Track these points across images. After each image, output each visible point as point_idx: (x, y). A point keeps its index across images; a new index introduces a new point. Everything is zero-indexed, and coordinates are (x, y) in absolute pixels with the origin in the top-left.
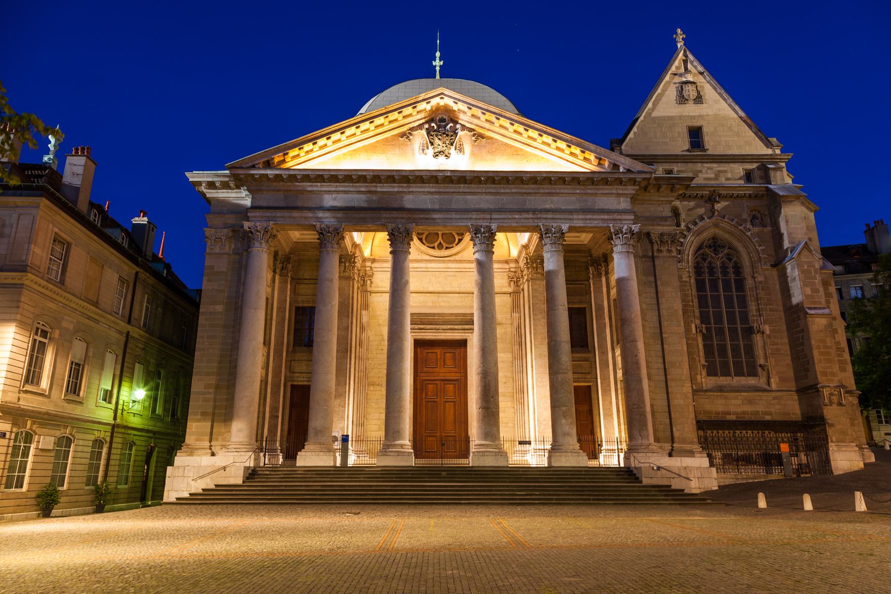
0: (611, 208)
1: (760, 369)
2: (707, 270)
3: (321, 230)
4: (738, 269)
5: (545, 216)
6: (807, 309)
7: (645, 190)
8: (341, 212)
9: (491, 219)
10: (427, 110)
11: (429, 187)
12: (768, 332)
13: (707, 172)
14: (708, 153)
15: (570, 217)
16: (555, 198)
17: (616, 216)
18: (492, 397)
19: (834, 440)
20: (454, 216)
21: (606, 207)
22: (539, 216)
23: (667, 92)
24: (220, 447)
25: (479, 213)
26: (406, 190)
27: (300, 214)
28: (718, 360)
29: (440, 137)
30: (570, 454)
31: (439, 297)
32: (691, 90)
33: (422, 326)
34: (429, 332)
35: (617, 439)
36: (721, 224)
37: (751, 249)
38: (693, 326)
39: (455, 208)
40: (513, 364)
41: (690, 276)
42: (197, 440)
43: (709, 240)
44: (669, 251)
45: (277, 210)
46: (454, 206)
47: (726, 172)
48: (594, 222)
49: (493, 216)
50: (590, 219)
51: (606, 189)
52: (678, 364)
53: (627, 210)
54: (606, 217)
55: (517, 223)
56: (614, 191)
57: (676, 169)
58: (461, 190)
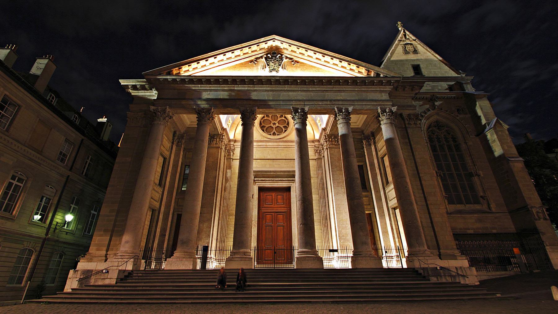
4: (454, 139)
7: (396, 90)
9: (305, 105)
10: (266, 48)
12: (482, 176)
16: (343, 94)
18: (309, 217)
19: (548, 244)
20: (281, 103)
21: (374, 98)
22: (334, 103)
23: (397, 49)
25: (297, 101)
26: (252, 89)
29: (273, 61)
30: (369, 258)
31: (273, 162)
32: (410, 48)
33: (263, 179)
34: (267, 183)
35: (398, 247)
36: (440, 113)
40: (319, 201)
42: (98, 250)
46: (281, 98)
47: (437, 86)
48: (367, 106)
50: (365, 105)
51: (373, 88)
54: (375, 103)
56: (378, 89)
58: (286, 89)
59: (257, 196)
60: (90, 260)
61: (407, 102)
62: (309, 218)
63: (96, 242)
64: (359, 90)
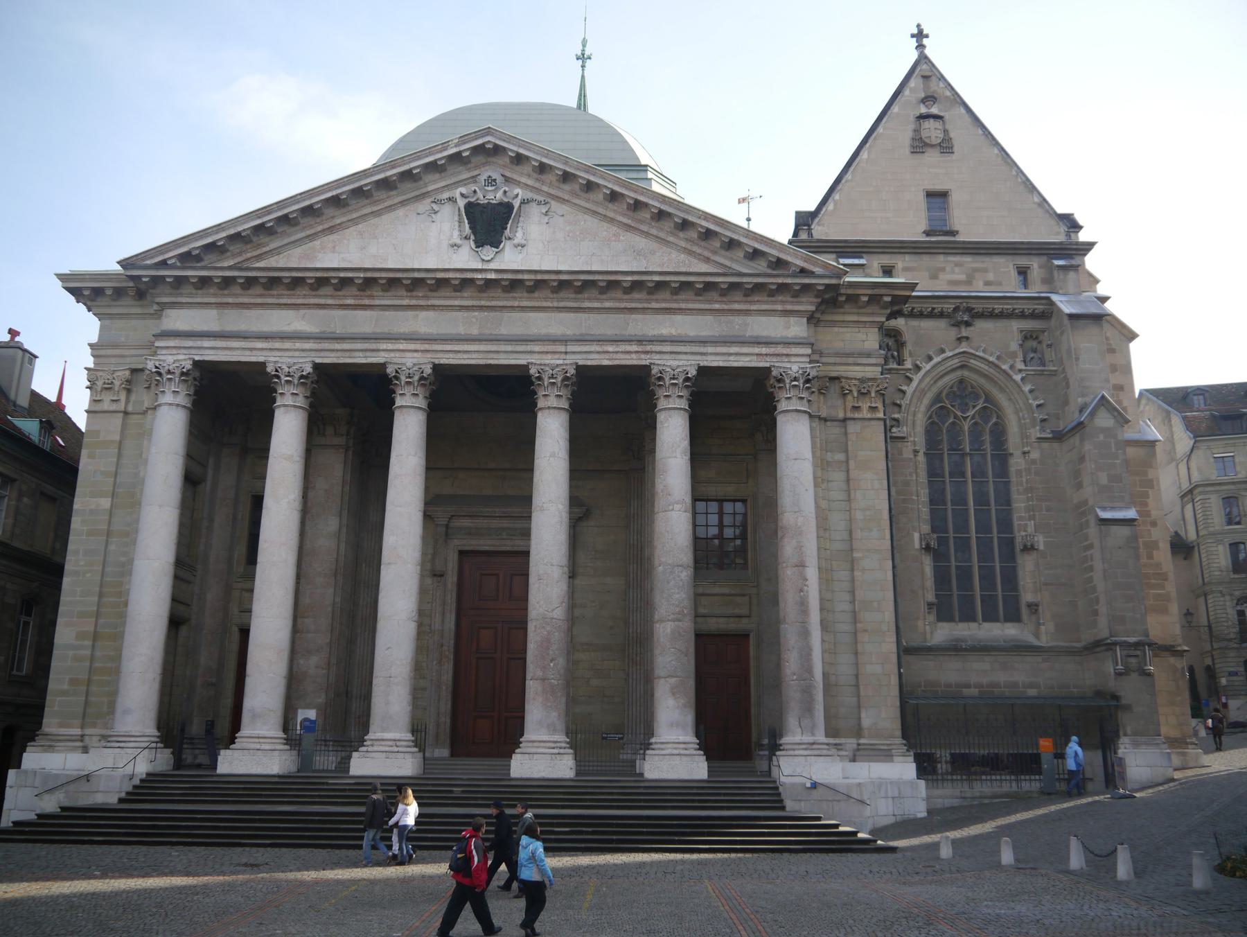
0: (773, 335)
1: (1024, 612)
2: (945, 437)
3: (277, 371)
5: (658, 348)
6: (1098, 510)
8: (312, 341)
9: (566, 353)
11: (462, 297)
12: (1042, 547)
13: (953, 272)
14: (959, 238)
15: (702, 350)
17: (780, 350)
18: (552, 661)
19: (1129, 731)
22: (648, 348)
24: (98, 738)
25: (547, 343)
26: (422, 302)
27: (243, 343)
28: (955, 592)
37: (1022, 405)
38: (916, 536)
39: (505, 333)
41: (916, 452)
42: (61, 725)
43: (951, 387)
44: (873, 409)
45: (205, 338)
48: (743, 358)
49: (570, 348)
50: (736, 354)
52: (875, 604)
53: (801, 338)
54: (764, 350)
55: (610, 359)
56: (779, 307)
57: (900, 265)
58: (516, 304)
59: (455, 579)
60: (50, 748)
61: (864, 341)
62: (552, 664)
63: (56, 708)
64: (726, 307)
